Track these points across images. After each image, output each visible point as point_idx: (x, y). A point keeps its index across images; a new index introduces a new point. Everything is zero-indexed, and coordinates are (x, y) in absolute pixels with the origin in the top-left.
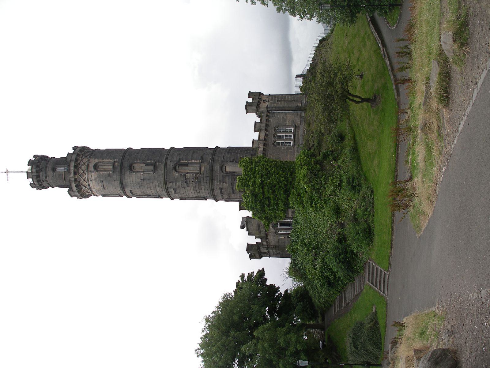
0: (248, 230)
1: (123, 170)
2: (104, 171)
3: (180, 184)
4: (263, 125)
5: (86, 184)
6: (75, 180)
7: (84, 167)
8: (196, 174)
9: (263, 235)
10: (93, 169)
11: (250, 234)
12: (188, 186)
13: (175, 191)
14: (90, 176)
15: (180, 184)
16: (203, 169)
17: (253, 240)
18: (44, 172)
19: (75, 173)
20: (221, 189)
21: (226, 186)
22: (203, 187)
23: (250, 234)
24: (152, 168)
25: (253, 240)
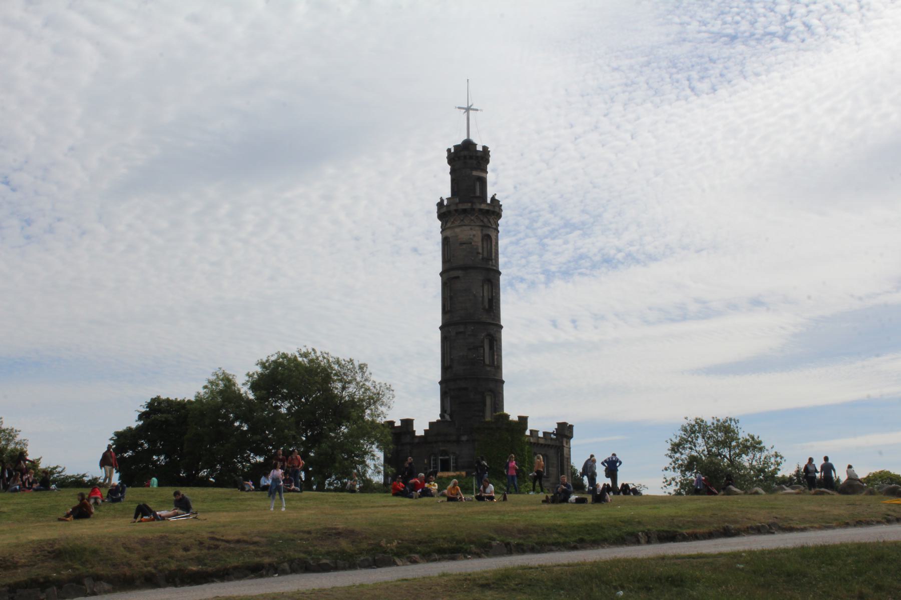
0: (438, 421)
2: (483, 248)
4: (549, 442)
5: (466, 222)
6: (473, 209)
7: (485, 220)
8: (484, 360)
10: (484, 232)
11: (431, 424)
13: (461, 333)
14: (477, 228)
16: (489, 369)
17: (420, 429)
18: (468, 162)
19: (481, 210)
23: (431, 424)
24: (487, 307)
25: (420, 429)
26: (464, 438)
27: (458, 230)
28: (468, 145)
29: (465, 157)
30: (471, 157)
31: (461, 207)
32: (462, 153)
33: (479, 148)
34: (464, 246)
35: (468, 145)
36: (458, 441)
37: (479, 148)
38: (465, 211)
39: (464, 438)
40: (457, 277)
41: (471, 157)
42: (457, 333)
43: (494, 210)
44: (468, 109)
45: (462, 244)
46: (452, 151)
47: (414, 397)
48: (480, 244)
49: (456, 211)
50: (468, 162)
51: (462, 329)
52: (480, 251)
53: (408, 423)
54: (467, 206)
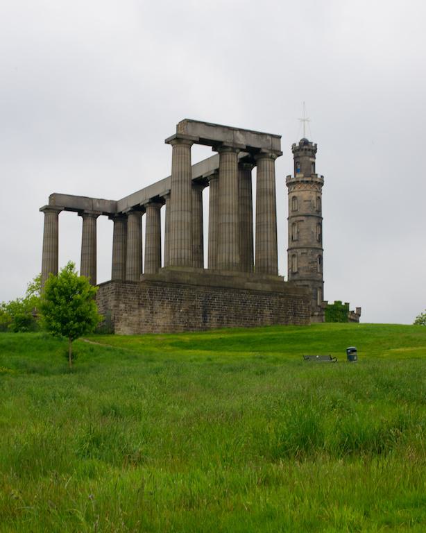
1: (317, 219)
3: (311, 258)
6: (312, 181)
12: (309, 263)
15: (311, 258)
19: (316, 182)
20: (308, 286)
21: (311, 290)
22: (309, 273)
26: (317, 314)
27: (302, 192)
28: (305, 142)
29: (306, 149)
30: (309, 150)
31: (305, 179)
32: (305, 147)
33: (313, 145)
34: (307, 203)
35: (305, 142)
37: (313, 145)
38: (307, 182)
39: (317, 314)
40: (303, 221)
41: (309, 150)
42: (302, 253)
45: (305, 201)
46: (297, 145)
48: (315, 202)
49: (302, 181)
51: (305, 251)
52: (315, 206)
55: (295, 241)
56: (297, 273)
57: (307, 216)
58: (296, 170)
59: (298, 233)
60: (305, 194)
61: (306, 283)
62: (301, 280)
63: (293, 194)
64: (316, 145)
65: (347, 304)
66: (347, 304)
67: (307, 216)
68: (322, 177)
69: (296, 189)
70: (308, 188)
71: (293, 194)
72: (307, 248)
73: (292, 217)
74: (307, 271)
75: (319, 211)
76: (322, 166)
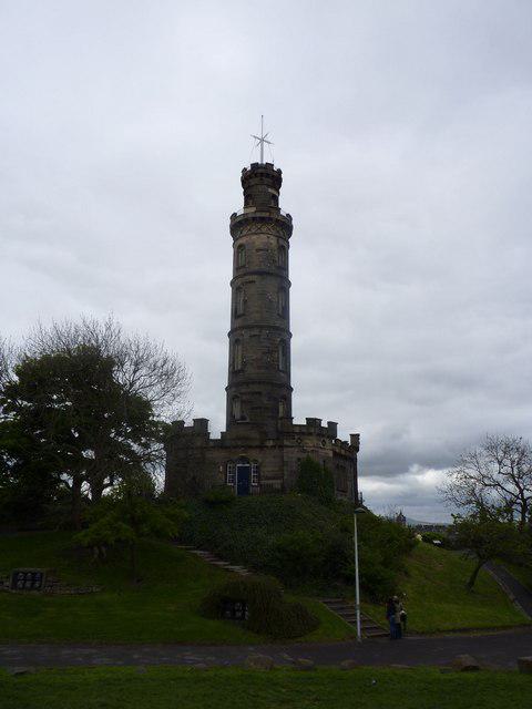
6: (270, 219)
9: (228, 443)
16: (282, 375)
18: (261, 182)
19: (277, 221)
20: (260, 393)
26: (271, 443)
27: (255, 237)
31: (258, 215)
32: (260, 171)
36: (261, 447)
39: (271, 443)
43: (285, 226)
44: (262, 140)
45: (258, 250)
47: (202, 398)
49: (254, 219)
50: (261, 182)
51: (256, 332)
53: (202, 424)
54: (266, 215)
55: (239, 316)
56: (242, 370)
57: (260, 273)
58: (247, 204)
59: (245, 302)
60: (262, 239)
61: (256, 388)
62: (247, 384)
63: (240, 242)
64: (279, 172)
65: (333, 426)
66: (333, 426)
67: (260, 273)
68: (288, 215)
69: (244, 233)
70: (264, 229)
71: (240, 242)
72: (261, 327)
73: (240, 276)
74: (259, 367)
75: (284, 267)
76: (287, 203)
